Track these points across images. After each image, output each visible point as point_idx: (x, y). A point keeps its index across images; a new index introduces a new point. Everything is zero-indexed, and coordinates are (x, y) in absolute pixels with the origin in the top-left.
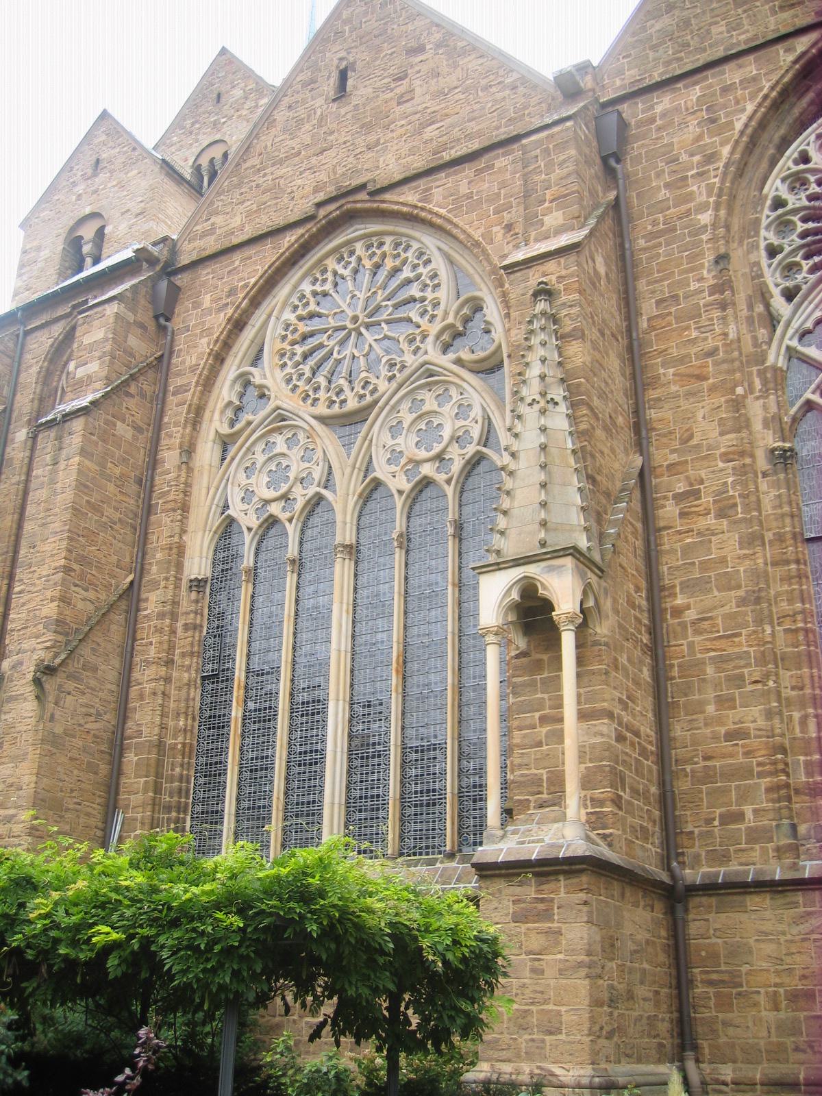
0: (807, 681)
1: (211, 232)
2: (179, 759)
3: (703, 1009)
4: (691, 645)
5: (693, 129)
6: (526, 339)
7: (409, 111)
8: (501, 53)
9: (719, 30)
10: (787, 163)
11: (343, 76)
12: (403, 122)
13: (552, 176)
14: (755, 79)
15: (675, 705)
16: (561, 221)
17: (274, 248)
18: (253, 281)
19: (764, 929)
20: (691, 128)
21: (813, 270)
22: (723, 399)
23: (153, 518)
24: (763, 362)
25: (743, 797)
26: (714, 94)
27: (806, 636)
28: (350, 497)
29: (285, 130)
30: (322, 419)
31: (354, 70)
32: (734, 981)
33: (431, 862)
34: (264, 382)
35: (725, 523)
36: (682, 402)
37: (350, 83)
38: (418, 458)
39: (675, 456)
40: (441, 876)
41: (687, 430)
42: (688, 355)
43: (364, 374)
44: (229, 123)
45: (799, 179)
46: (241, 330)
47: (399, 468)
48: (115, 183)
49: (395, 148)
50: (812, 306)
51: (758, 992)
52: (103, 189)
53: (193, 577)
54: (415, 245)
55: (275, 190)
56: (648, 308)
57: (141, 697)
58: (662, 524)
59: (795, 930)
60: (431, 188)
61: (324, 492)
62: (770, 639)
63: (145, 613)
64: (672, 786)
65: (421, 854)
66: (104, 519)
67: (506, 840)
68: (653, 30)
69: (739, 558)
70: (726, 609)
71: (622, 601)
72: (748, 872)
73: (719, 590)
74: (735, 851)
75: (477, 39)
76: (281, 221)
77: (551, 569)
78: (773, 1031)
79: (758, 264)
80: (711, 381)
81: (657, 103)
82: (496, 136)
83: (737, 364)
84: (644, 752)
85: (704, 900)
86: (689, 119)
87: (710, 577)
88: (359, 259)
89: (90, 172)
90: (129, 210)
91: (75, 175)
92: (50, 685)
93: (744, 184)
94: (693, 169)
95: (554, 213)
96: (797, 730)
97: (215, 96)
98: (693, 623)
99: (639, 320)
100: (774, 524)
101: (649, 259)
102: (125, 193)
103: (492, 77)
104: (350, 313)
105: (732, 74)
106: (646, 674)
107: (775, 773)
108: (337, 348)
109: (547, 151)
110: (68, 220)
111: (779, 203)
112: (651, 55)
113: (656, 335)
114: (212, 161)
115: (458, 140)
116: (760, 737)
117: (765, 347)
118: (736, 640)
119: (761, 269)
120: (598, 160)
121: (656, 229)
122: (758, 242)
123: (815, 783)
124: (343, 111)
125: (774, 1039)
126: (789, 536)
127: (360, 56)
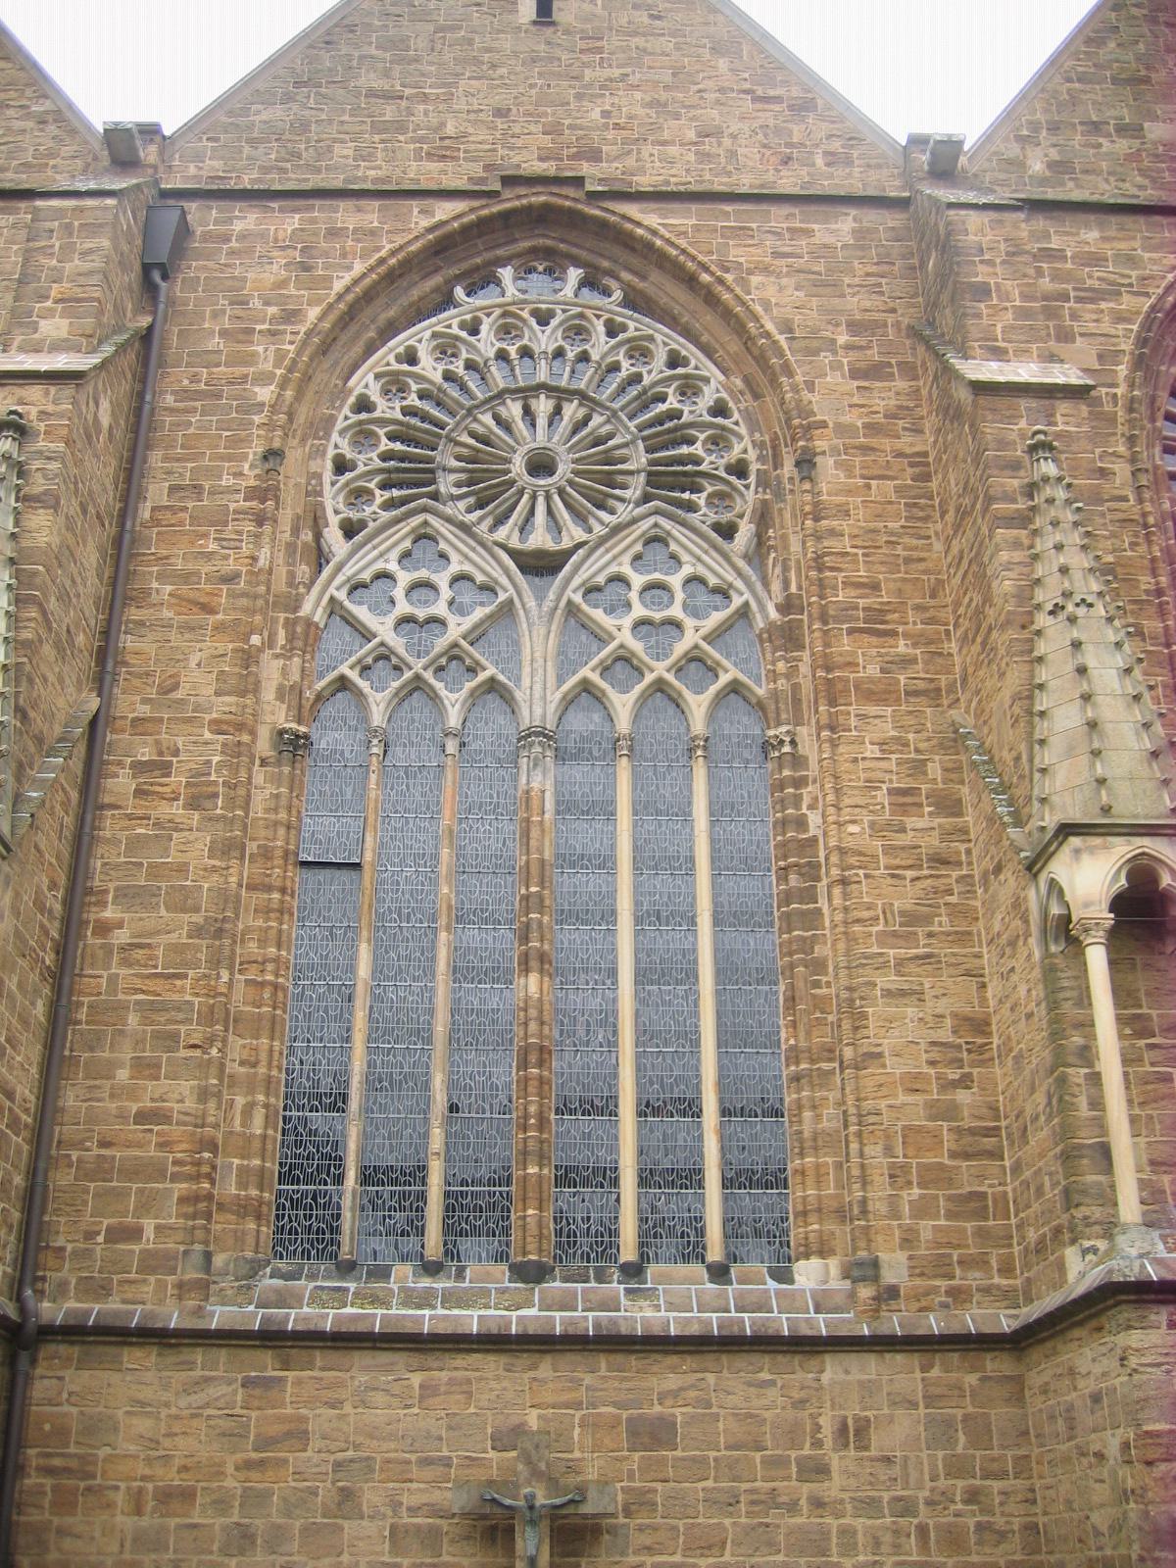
0: (263, 1056)
3: (32, 1510)
4: (113, 980)
5: (275, 271)
8: (35, 66)
9: (344, 151)
10: (387, 356)
13: (67, 265)
14: (373, 233)
15: (74, 1061)
16: (64, 334)
19: (141, 1396)
20: (275, 266)
21: (389, 505)
22: (231, 646)
24: (296, 609)
25: (145, 1206)
26: (315, 234)
27: (274, 994)
32: (84, 1469)
35: (196, 817)
36: (173, 635)
39: (147, 708)
42: (197, 573)
45: (397, 382)
50: (376, 553)
51: (117, 1488)
56: (156, 492)
58: (107, 800)
59: (183, 1402)
64: (46, 1178)
68: (257, 118)
69: (205, 870)
70: (173, 938)
71: (28, 898)
74: (121, 1283)
78: (128, 1545)
79: (319, 476)
80: (220, 617)
81: (237, 217)
83: (260, 602)
84: (14, 1124)
85: (63, 1349)
86: (275, 253)
93: (326, 365)
94: (263, 322)
95: (57, 320)
96: (237, 1122)
98: (123, 949)
99: (141, 505)
100: (263, 833)
103: (13, 95)
105: (346, 215)
106: (40, 1010)
107: (196, 1178)
109: (68, 227)
111: (364, 405)
112: (247, 150)
113: (158, 533)
116: (185, 1124)
117: (302, 590)
118: (178, 983)
119: (321, 484)
120: (137, 267)
121: (194, 387)
122: (325, 447)
123: (248, 1198)
125: (127, 1556)
126: (279, 853)
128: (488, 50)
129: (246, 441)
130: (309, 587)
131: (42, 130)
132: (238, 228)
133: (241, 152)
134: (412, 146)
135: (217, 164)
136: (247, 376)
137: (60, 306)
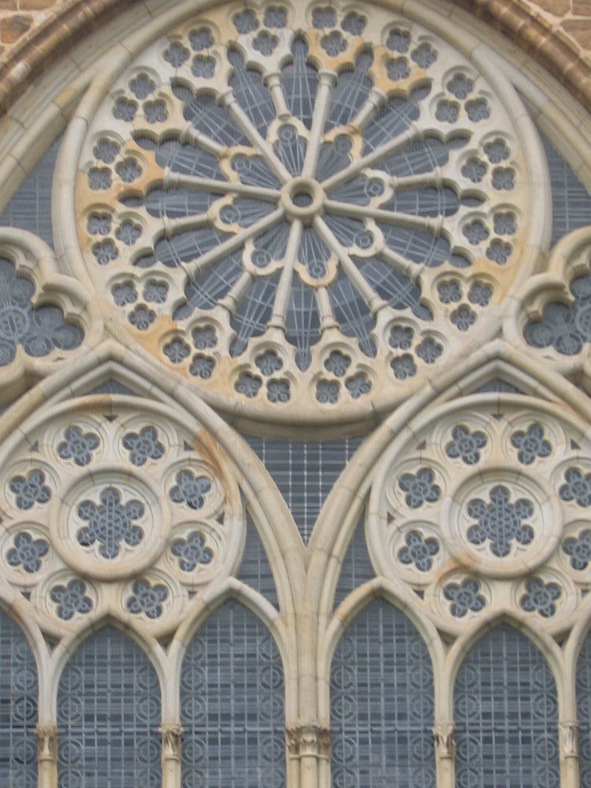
18: (39, 19)
28: (323, 620)
30: (233, 417)
88: (300, 39)
108: (250, 249)
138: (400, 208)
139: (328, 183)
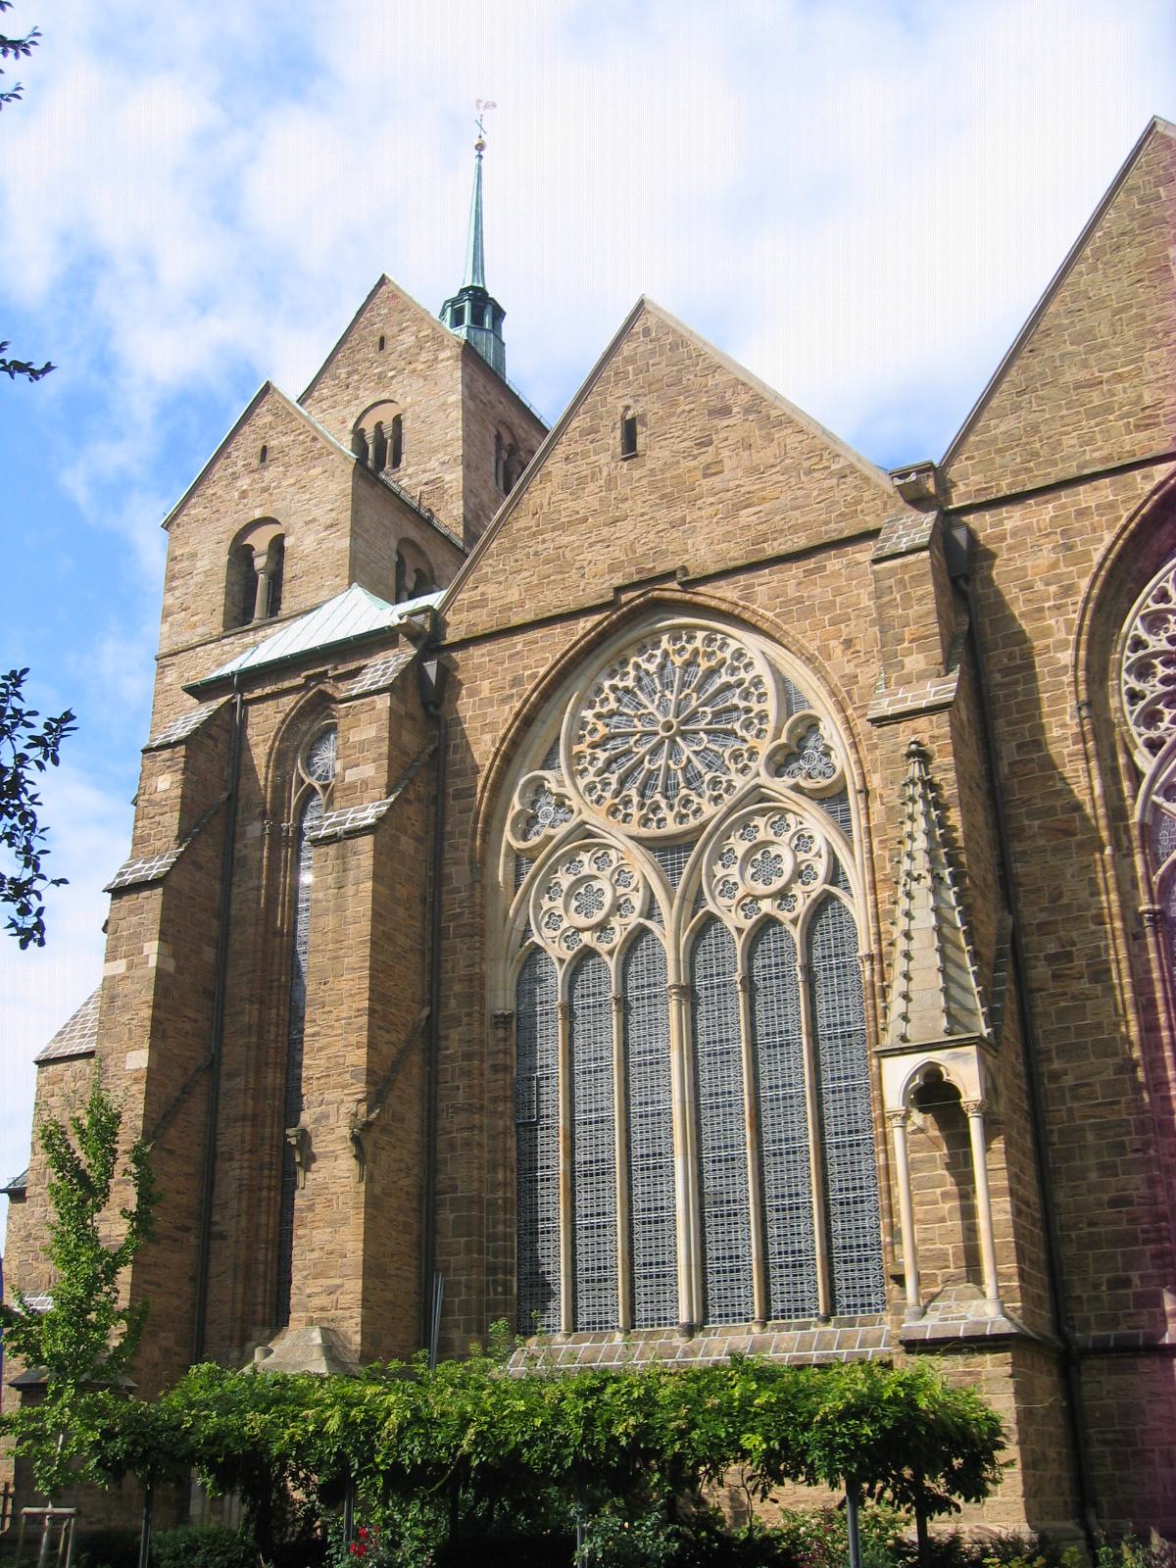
1: (482, 603)
2: (501, 1216)
4: (1070, 1110)
5: (1046, 556)
6: (903, 804)
7: (719, 486)
11: (630, 430)
12: (712, 500)
13: (910, 611)
14: (1112, 506)
16: (922, 666)
17: (566, 634)
18: (542, 671)
20: (1045, 552)
23: (445, 943)
29: (564, 487)
31: (645, 425)
33: (805, 1326)
34: (561, 790)
37: (641, 440)
38: (757, 893)
39: (1044, 914)
40: (819, 1341)
41: (1055, 889)
42: (1052, 808)
43: (684, 792)
44: (400, 378)
46: (529, 726)
47: (734, 902)
48: (292, 481)
49: (705, 530)
51: (1152, 1451)
52: (275, 488)
53: (499, 1012)
54: (733, 645)
55: (560, 563)
56: (1008, 752)
57: (452, 1147)
58: (1034, 985)
60: (752, 585)
61: (649, 924)
62: (1148, 1108)
63: (448, 1052)
65: (790, 1317)
66: (399, 950)
67: (927, 1316)
68: (998, 431)
70: (1104, 1077)
71: (1009, 1074)
72: (1137, 1336)
73: (1096, 1057)
75: (795, 409)
76: (571, 603)
77: (956, 1056)
82: (826, 533)
85: (1096, 1363)
86: (1042, 541)
87: (1086, 1043)
88: (666, 654)
89: (255, 462)
90: (314, 520)
91: (235, 464)
92: (367, 1144)
94: (1048, 600)
97: (377, 339)
101: (1007, 696)
102: (308, 496)
104: (661, 719)
105: (1085, 495)
107: (1159, 1240)
108: (647, 757)
109: (901, 581)
110: (231, 525)
111: (1138, 644)
112: (998, 460)
113: (1019, 782)
114: (379, 425)
115: (782, 531)
118: (1116, 1107)
119: (1124, 717)
124: (636, 474)
127: (646, 406)
128: (1158, 320)
129: (1062, 698)
130: (1135, 797)
131: (845, 483)
132: (1009, 527)
133: (993, 463)
134: (1121, 423)
135: (978, 478)
136: (1048, 646)
137: (914, 645)
138: (716, 723)
139: (671, 715)
